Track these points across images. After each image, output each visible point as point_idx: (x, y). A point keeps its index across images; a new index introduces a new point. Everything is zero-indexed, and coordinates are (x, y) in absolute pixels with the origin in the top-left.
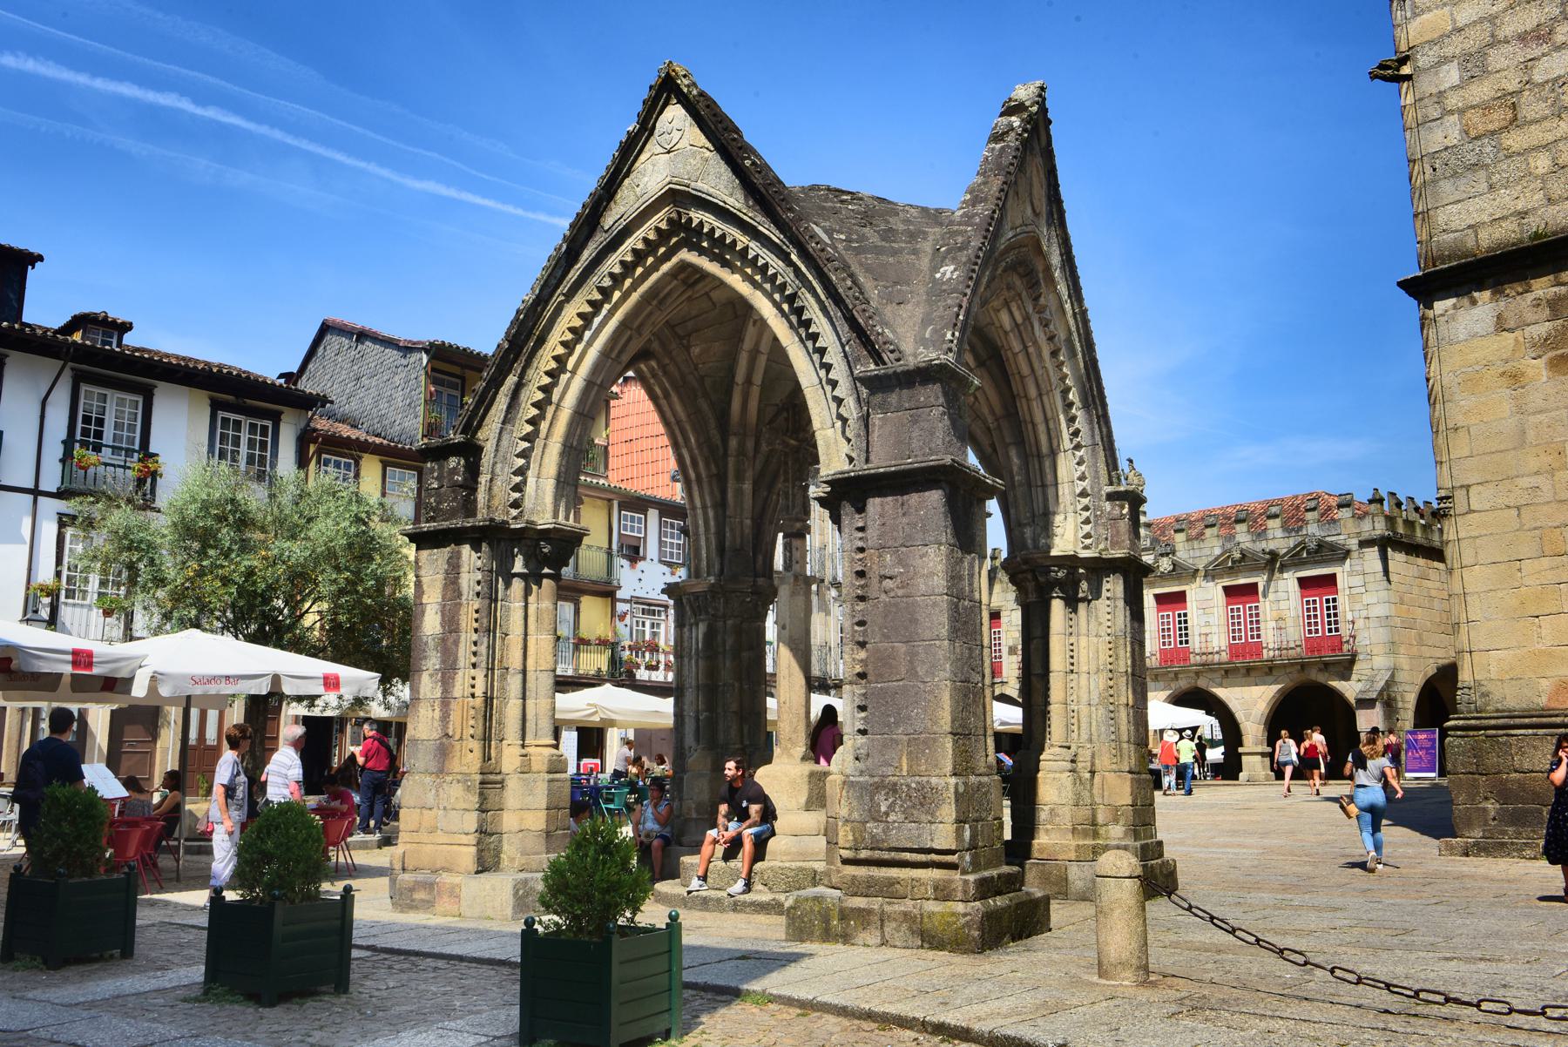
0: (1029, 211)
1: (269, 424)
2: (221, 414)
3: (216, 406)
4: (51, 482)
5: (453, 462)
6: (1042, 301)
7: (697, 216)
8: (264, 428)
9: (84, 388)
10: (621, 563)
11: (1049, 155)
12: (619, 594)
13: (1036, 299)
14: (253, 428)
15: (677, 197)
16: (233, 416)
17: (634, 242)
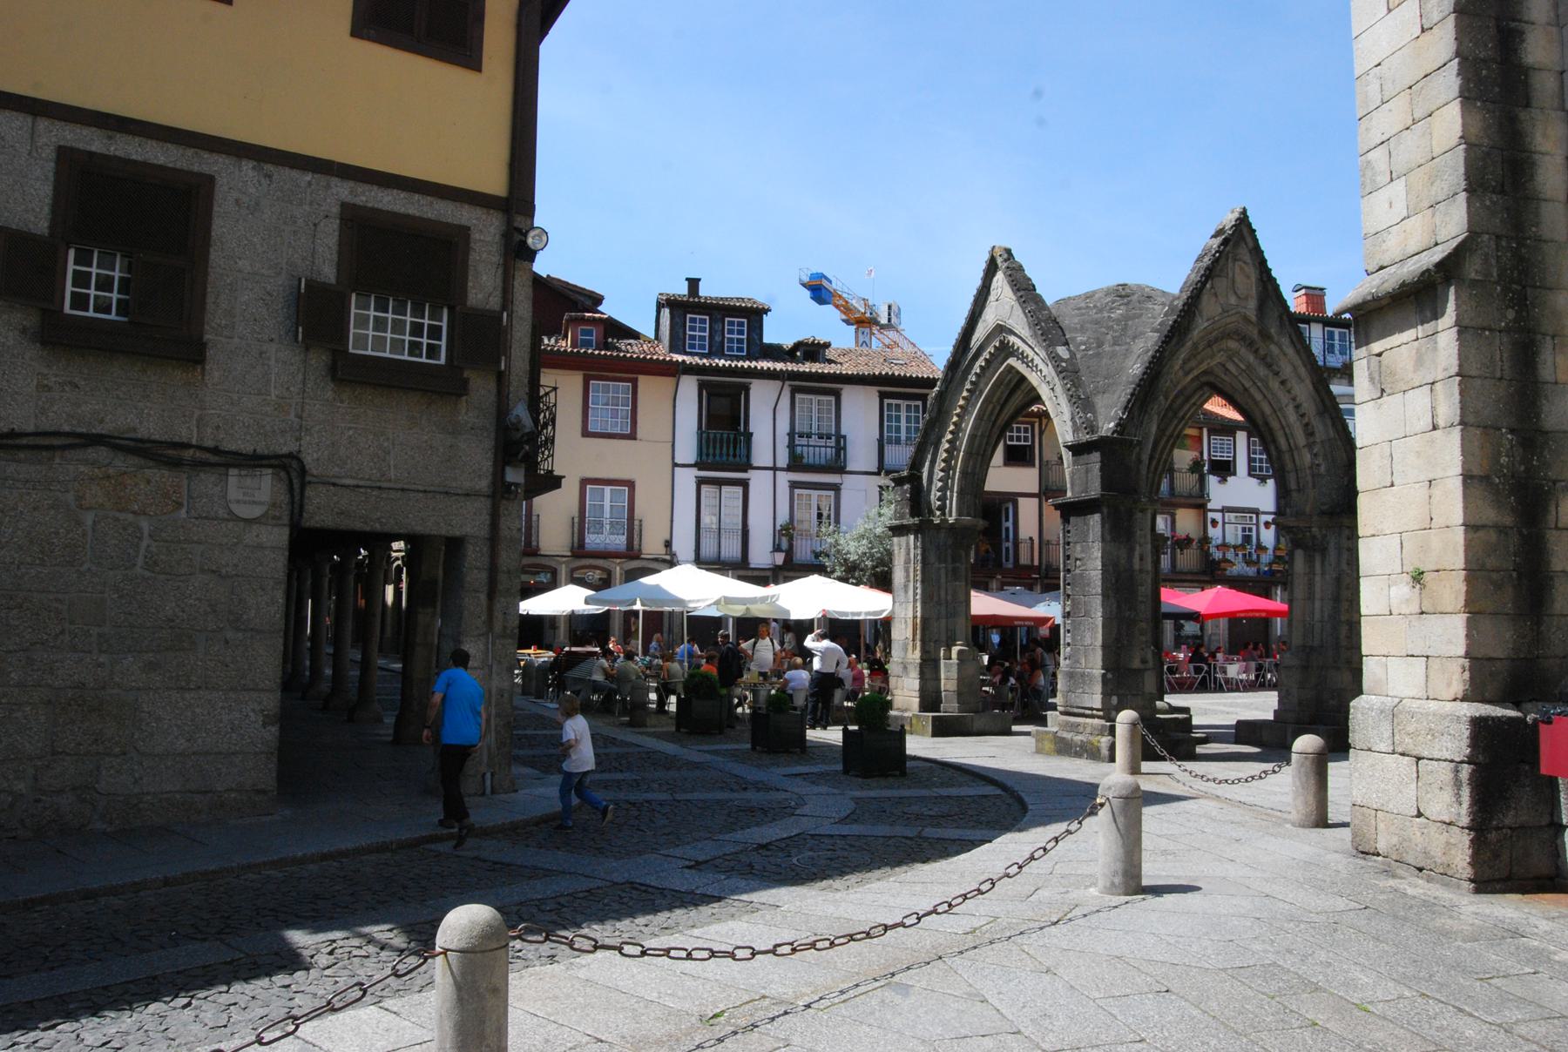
0: (1233, 300)
1: (920, 403)
2: (886, 401)
3: (882, 396)
4: (783, 461)
5: (907, 487)
6: (1262, 352)
7: (1012, 339)
8: (917, 407)
9: (798, 396)
10: (1212, 480)
11: (1257, 252)
12: (1210, 506)
13: (1256, 351)
14: (909, 407)
15: (1000, 329)
16: (894, 402)
17: (986, 355)
